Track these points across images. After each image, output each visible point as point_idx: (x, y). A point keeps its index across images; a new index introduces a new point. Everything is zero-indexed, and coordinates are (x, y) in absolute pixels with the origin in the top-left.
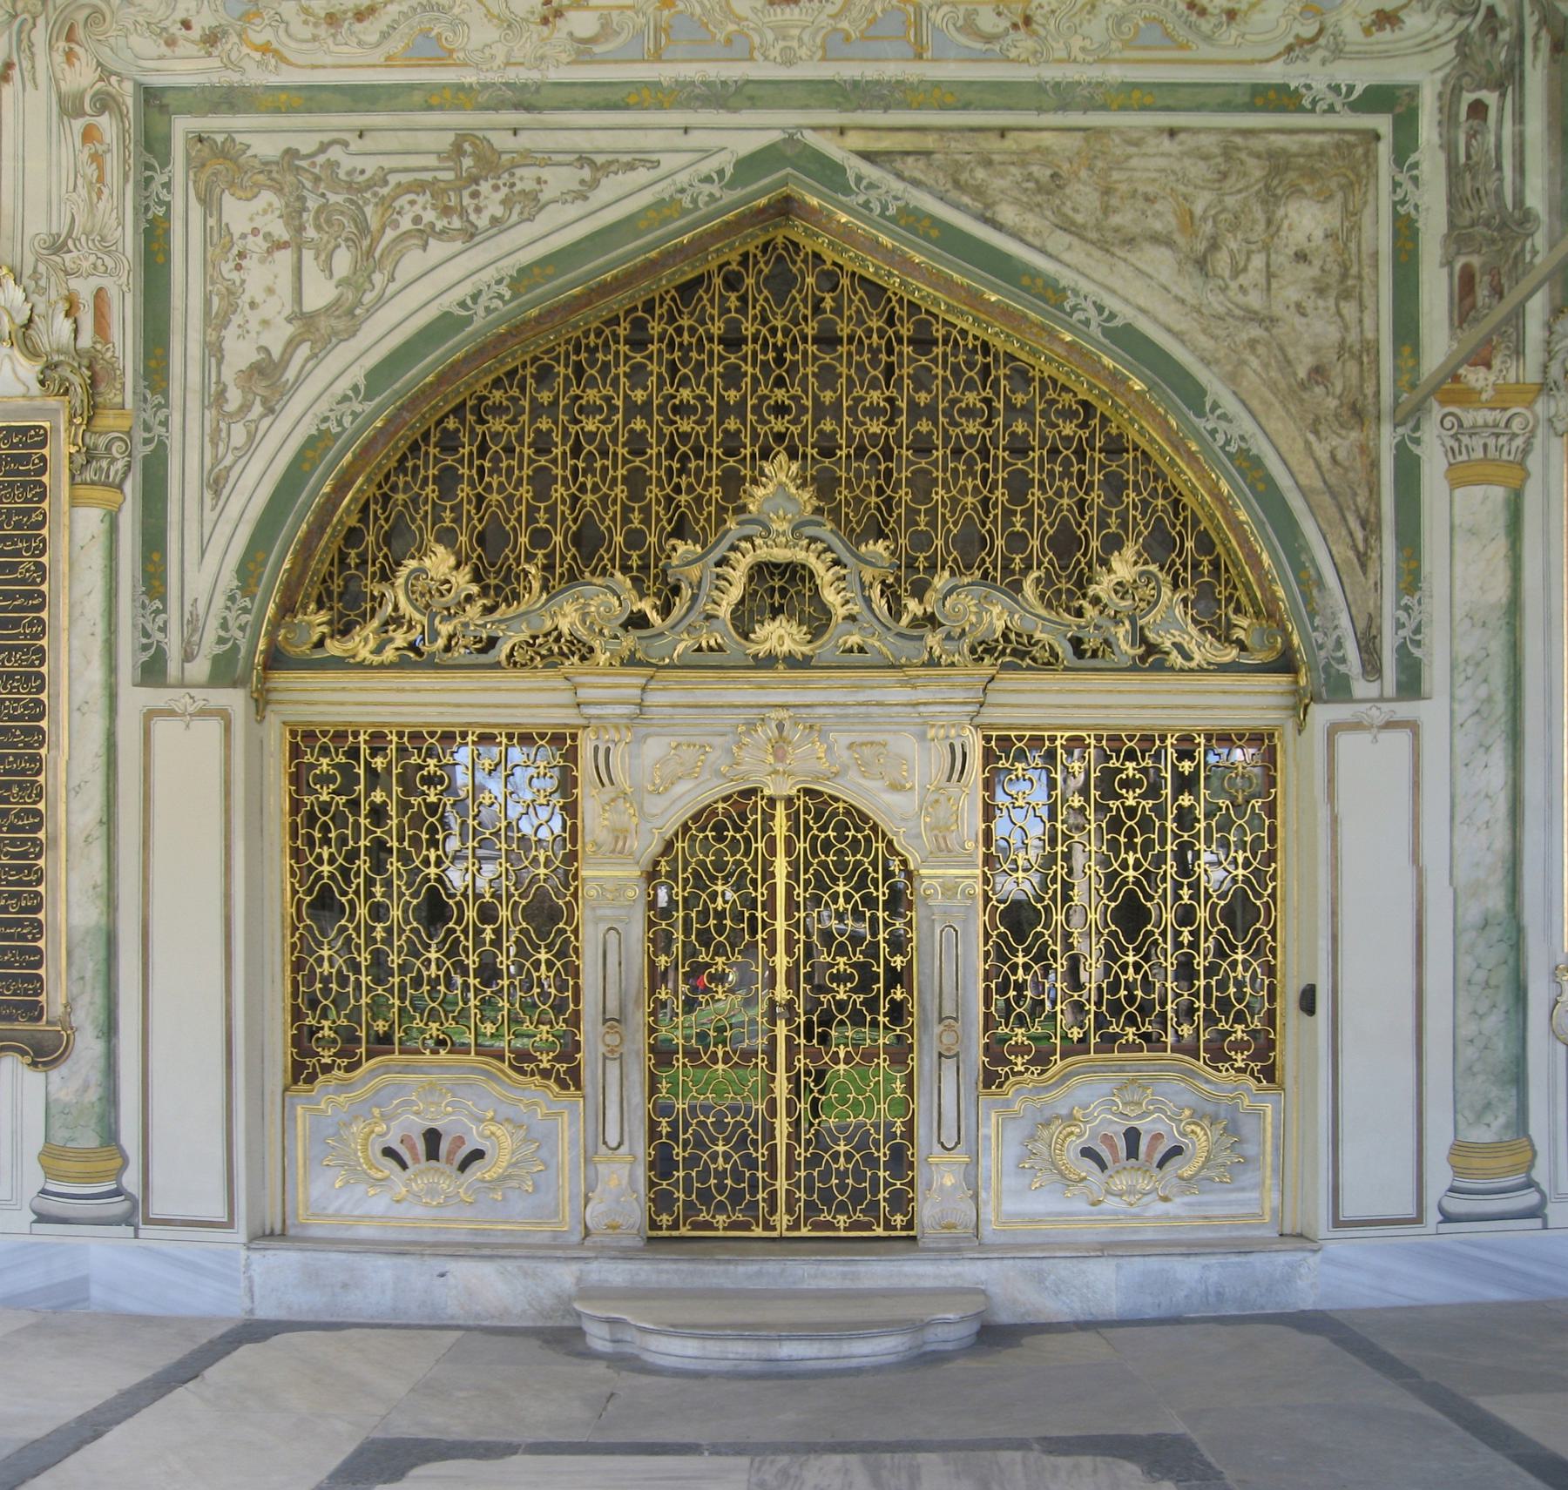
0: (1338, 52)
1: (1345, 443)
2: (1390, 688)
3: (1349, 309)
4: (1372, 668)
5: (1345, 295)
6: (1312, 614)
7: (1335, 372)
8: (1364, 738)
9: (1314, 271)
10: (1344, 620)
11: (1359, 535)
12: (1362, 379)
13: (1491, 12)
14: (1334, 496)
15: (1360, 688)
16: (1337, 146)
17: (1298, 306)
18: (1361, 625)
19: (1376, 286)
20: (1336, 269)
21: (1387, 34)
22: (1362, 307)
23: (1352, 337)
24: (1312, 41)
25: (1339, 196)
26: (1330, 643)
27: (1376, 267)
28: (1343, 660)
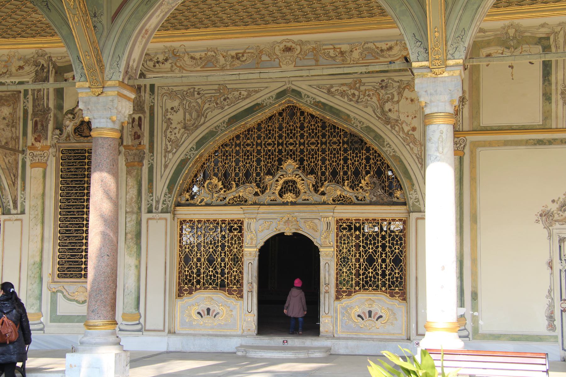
0: (11, 75)
1: (11, 159)
2: (19, 212)
3: (13, 129)
4: (15, 207)
5: (13, 126)
6: (3, 195)
7: (10, 143)
8: (11, 222)
9: (7, 122)
10: (10, 197)
11: (13, 178)
12: (15, 144)
13: (43, 65)
14: (8, 170)
15: (13, 211)
16: (12, 94)
17: (3, 129)
18: (13, 197)
19: (19, 124)
20: (11, 121)
21: (21, 71)
22: (16, 129)
23: (14, 135)
24: (5, 73)
25: (12, 105)
26: (7, 202)
27: (19, 120)
28: (9, 205)
